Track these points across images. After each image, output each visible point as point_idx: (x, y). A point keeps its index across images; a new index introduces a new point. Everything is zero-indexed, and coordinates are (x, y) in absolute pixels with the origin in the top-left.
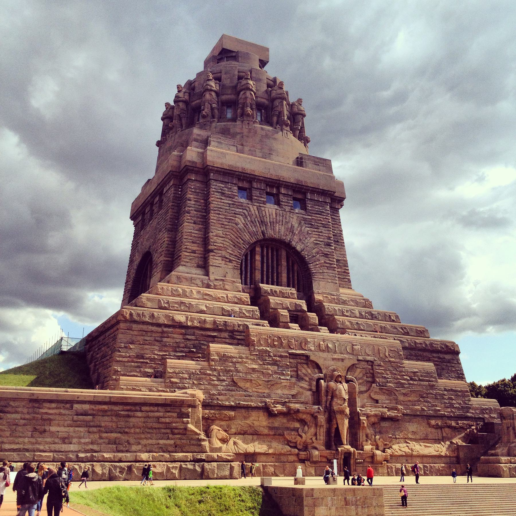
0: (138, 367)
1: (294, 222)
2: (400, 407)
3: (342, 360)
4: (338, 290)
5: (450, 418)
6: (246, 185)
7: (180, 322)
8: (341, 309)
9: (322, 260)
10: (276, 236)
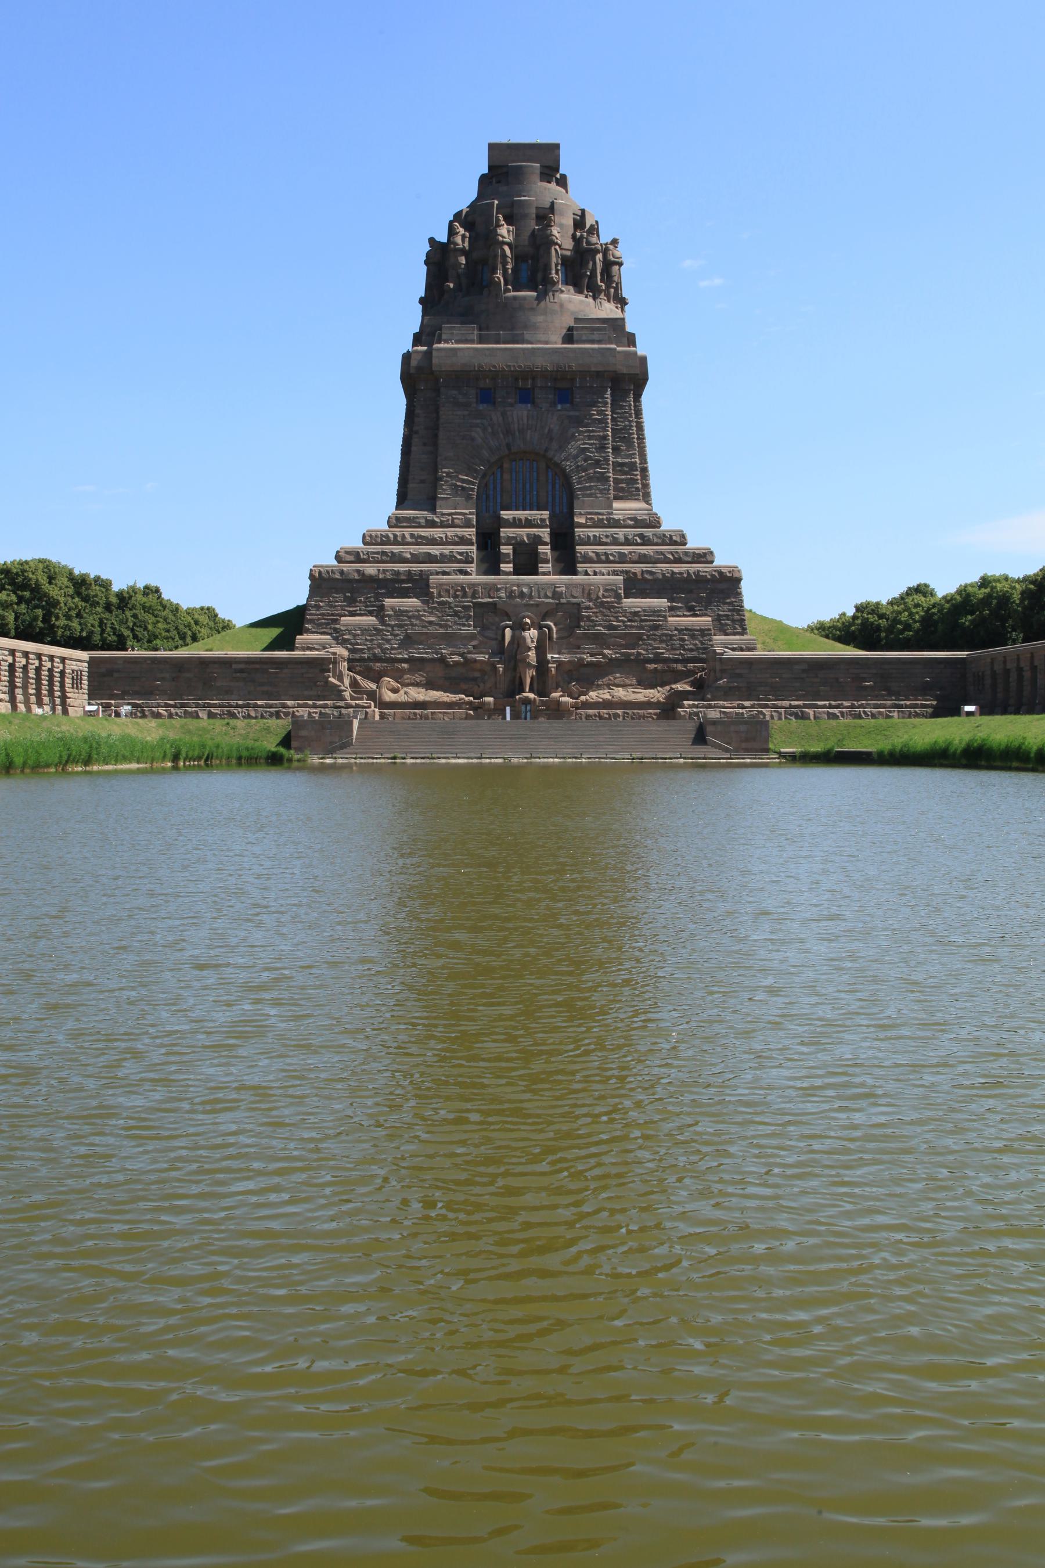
0: (328, 624)
2: (606, 651)
3: (537, 605)
4: (610, 507)
5: (676, 661)
7: (371, 576)
8: (597, 534)
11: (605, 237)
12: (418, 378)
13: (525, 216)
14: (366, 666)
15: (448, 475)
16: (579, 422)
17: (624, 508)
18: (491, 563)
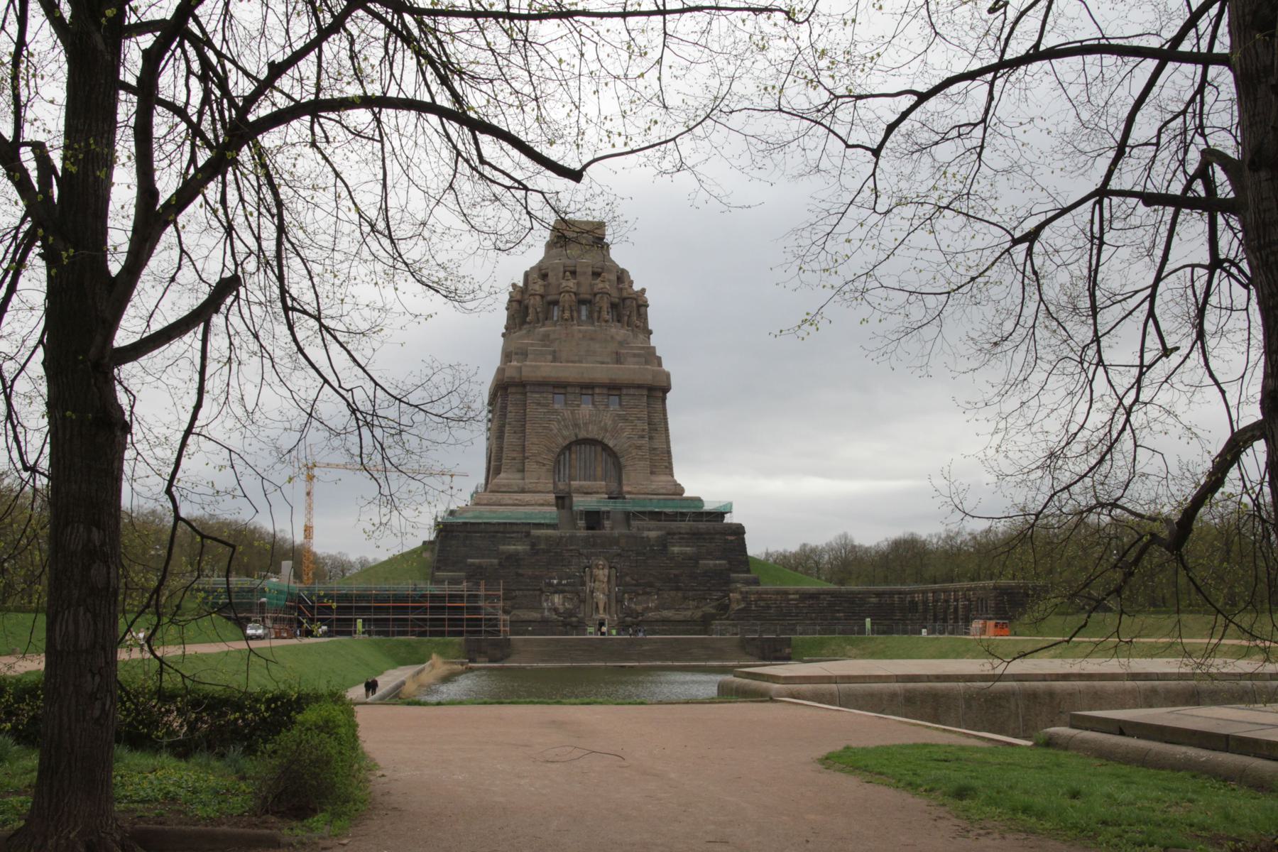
1: (608, 420)
6: (562, 391)
9: (634, 452)
10: (589, 436)
11: (636, 287)
13: (585, 273)
15: (534, 455)
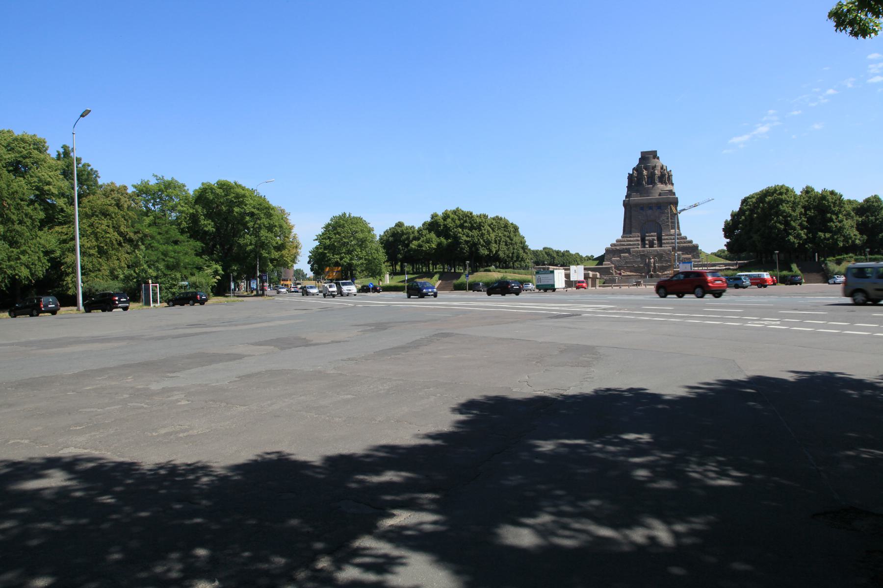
12: (625, 204)
14: (617, 268)
16: (663, 213)
17: (672, 231)
18: (644, 246)
